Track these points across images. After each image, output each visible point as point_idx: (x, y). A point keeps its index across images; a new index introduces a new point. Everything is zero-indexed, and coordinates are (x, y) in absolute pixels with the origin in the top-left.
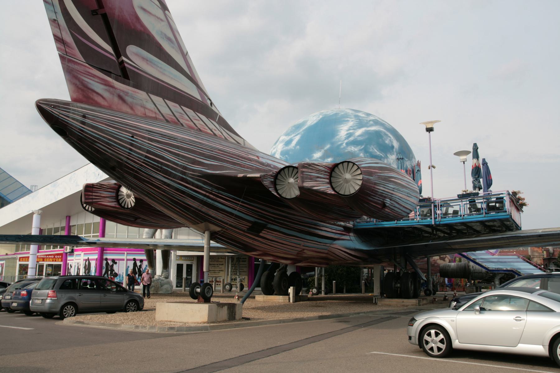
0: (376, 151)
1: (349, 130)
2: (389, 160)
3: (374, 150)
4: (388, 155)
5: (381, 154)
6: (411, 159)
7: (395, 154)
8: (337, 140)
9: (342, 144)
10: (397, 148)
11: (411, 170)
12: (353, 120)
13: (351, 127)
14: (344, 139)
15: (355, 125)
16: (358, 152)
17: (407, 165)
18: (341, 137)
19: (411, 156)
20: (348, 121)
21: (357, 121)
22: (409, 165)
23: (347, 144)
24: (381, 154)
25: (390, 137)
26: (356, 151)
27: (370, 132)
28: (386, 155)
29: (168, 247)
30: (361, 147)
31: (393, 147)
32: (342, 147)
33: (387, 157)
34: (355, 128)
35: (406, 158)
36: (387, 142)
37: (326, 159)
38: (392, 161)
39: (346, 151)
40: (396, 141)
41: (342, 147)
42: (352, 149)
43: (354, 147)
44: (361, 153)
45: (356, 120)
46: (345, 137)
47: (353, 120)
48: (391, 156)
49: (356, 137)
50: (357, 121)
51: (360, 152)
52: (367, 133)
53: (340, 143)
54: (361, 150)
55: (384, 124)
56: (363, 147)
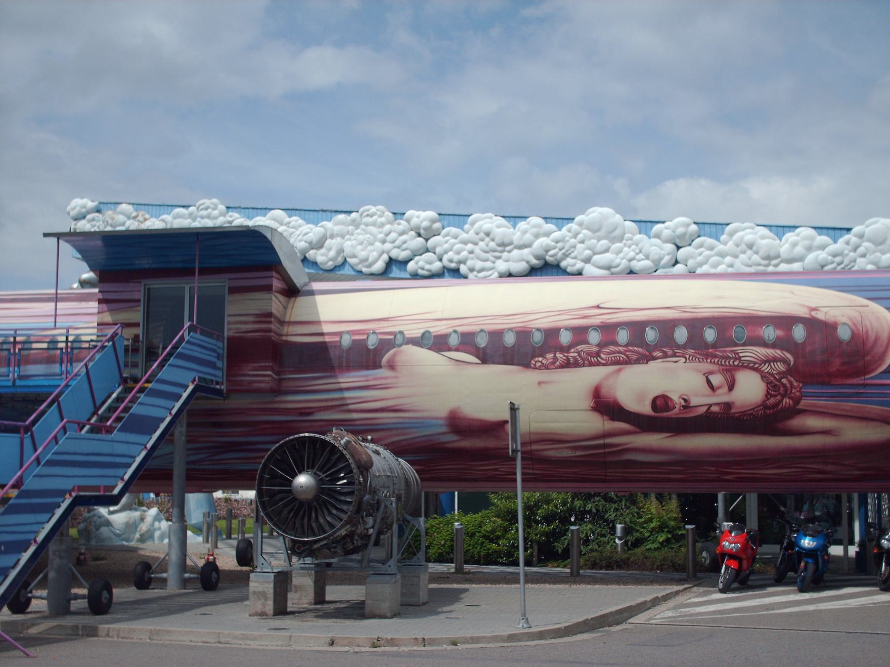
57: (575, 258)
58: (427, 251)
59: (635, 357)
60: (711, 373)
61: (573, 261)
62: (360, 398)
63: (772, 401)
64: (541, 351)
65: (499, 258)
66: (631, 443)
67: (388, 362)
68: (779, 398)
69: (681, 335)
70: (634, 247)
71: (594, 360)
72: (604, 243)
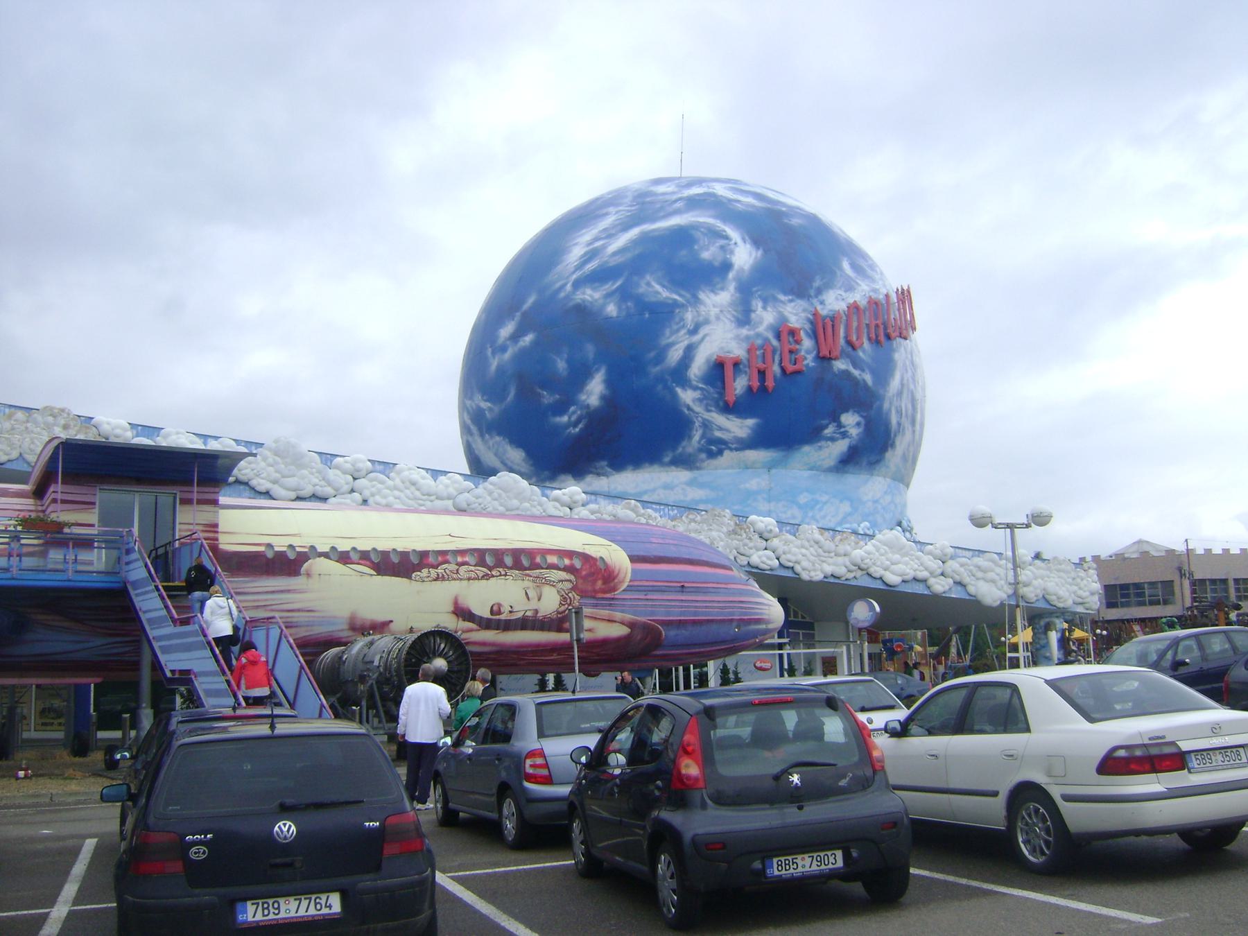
0: (658, 288)
1: (596, 239)
2: (702, 308)
3: (653, 286)
4: (702, 296)
5: (676, 297)
6: (812, 292)
7: (732, 287)
8: (556, 276)
9: (565, 285)
10: (747, 267)
11: (808, 326)
12: (621, 208)
13: (605, 230)
14: (572, 270)
15: (617, 222)
16: (601, 301)
17: (786, 313)
18: (567, 265)
19: (817, 283)
20: (607, 214)
21: (633, 208)
22: (796, 314)
23: (577, 284)
24: (676, 297)
25: (727, 238)
26: (596, 301)
27: (656, 233)
28: (695, 297)
29: (291, 622)
30: (613, 285)
31: (727, 266)
32: (562, 295)
33: (696, 301)
34: (613, 232)
35: (785, 294)
36: (706, 255)
37: (521, 339)
38: (714, 312)
39: (571, 304)
40: (748, 246)
41: (562, 295)
42: (586, 296)
43: (594, 289)
44: (609, 303)
45: (634, 205)
46: (576, 264)
47: (621, 208)
48: (712, 296)
49: (606, 259)
50: (633, 208)
51: (608, 300)
52: (644, 239)
53: (558, 285)
54: (608, 295)
55: (730, 200)
56: (618, 283)
57: (878, 566)
58: (766, 549)
59: (481, 575)
60: (528, 588)
61: (877, 569)
62: (281, 599)
63: (563, 608)
64: (419, 567)
65: (823, 562)
66: (469, 638)
67: (307, 571)
68: (566, 606)
69: (508, 560)
70: (916, 561)
71: (455, 576)
72: (897, 557)
